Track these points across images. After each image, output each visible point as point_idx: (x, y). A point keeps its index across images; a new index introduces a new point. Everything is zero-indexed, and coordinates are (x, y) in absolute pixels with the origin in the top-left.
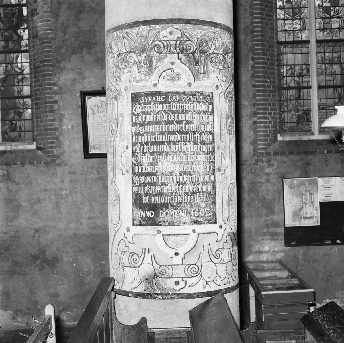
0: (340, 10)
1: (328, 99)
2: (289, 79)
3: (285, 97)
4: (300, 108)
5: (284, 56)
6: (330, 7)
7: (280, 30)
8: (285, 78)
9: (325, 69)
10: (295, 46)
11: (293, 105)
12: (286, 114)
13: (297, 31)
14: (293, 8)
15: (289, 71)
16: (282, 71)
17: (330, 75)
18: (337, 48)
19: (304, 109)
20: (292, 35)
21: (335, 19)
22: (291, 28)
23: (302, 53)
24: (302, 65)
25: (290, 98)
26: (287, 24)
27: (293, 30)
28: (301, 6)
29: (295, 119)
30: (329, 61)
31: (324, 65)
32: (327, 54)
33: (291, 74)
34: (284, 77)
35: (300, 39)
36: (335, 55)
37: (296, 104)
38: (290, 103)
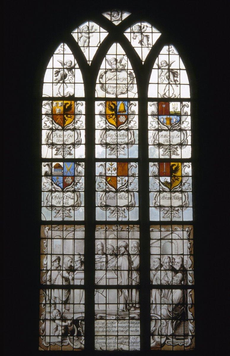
0: (130, 181)
1: (109, 304)
2: (55, 274)
3: (47, 299)
4: (69, 316)
5: (49, 241)
6: (117, 177)
7: (45, 205)
8: (50, 272)
9: (107, 262)
10: (64, 229)
11: (59, 311)
12: (48, 323)
13: (69, 208)
14: (64, 177)
16: (45, 262)
17: (113, 270)
18: (124, 234)
19: (75, 318)
20: (61, 212)
21: (123, 192)
23: (74, 239)
24: (74, 255)
25: (54, 301)
26: (56, 197)
27: (63, 207)
28: (76, 174)
29: (60, 331)
30: (113, 251)
31: (104, 256)
32: (110, 241)
33: (57, 267)
34: (47, 271)
35: (72, 219)
36: (121, 243)
37: (64, 310)
38: (55, 309)
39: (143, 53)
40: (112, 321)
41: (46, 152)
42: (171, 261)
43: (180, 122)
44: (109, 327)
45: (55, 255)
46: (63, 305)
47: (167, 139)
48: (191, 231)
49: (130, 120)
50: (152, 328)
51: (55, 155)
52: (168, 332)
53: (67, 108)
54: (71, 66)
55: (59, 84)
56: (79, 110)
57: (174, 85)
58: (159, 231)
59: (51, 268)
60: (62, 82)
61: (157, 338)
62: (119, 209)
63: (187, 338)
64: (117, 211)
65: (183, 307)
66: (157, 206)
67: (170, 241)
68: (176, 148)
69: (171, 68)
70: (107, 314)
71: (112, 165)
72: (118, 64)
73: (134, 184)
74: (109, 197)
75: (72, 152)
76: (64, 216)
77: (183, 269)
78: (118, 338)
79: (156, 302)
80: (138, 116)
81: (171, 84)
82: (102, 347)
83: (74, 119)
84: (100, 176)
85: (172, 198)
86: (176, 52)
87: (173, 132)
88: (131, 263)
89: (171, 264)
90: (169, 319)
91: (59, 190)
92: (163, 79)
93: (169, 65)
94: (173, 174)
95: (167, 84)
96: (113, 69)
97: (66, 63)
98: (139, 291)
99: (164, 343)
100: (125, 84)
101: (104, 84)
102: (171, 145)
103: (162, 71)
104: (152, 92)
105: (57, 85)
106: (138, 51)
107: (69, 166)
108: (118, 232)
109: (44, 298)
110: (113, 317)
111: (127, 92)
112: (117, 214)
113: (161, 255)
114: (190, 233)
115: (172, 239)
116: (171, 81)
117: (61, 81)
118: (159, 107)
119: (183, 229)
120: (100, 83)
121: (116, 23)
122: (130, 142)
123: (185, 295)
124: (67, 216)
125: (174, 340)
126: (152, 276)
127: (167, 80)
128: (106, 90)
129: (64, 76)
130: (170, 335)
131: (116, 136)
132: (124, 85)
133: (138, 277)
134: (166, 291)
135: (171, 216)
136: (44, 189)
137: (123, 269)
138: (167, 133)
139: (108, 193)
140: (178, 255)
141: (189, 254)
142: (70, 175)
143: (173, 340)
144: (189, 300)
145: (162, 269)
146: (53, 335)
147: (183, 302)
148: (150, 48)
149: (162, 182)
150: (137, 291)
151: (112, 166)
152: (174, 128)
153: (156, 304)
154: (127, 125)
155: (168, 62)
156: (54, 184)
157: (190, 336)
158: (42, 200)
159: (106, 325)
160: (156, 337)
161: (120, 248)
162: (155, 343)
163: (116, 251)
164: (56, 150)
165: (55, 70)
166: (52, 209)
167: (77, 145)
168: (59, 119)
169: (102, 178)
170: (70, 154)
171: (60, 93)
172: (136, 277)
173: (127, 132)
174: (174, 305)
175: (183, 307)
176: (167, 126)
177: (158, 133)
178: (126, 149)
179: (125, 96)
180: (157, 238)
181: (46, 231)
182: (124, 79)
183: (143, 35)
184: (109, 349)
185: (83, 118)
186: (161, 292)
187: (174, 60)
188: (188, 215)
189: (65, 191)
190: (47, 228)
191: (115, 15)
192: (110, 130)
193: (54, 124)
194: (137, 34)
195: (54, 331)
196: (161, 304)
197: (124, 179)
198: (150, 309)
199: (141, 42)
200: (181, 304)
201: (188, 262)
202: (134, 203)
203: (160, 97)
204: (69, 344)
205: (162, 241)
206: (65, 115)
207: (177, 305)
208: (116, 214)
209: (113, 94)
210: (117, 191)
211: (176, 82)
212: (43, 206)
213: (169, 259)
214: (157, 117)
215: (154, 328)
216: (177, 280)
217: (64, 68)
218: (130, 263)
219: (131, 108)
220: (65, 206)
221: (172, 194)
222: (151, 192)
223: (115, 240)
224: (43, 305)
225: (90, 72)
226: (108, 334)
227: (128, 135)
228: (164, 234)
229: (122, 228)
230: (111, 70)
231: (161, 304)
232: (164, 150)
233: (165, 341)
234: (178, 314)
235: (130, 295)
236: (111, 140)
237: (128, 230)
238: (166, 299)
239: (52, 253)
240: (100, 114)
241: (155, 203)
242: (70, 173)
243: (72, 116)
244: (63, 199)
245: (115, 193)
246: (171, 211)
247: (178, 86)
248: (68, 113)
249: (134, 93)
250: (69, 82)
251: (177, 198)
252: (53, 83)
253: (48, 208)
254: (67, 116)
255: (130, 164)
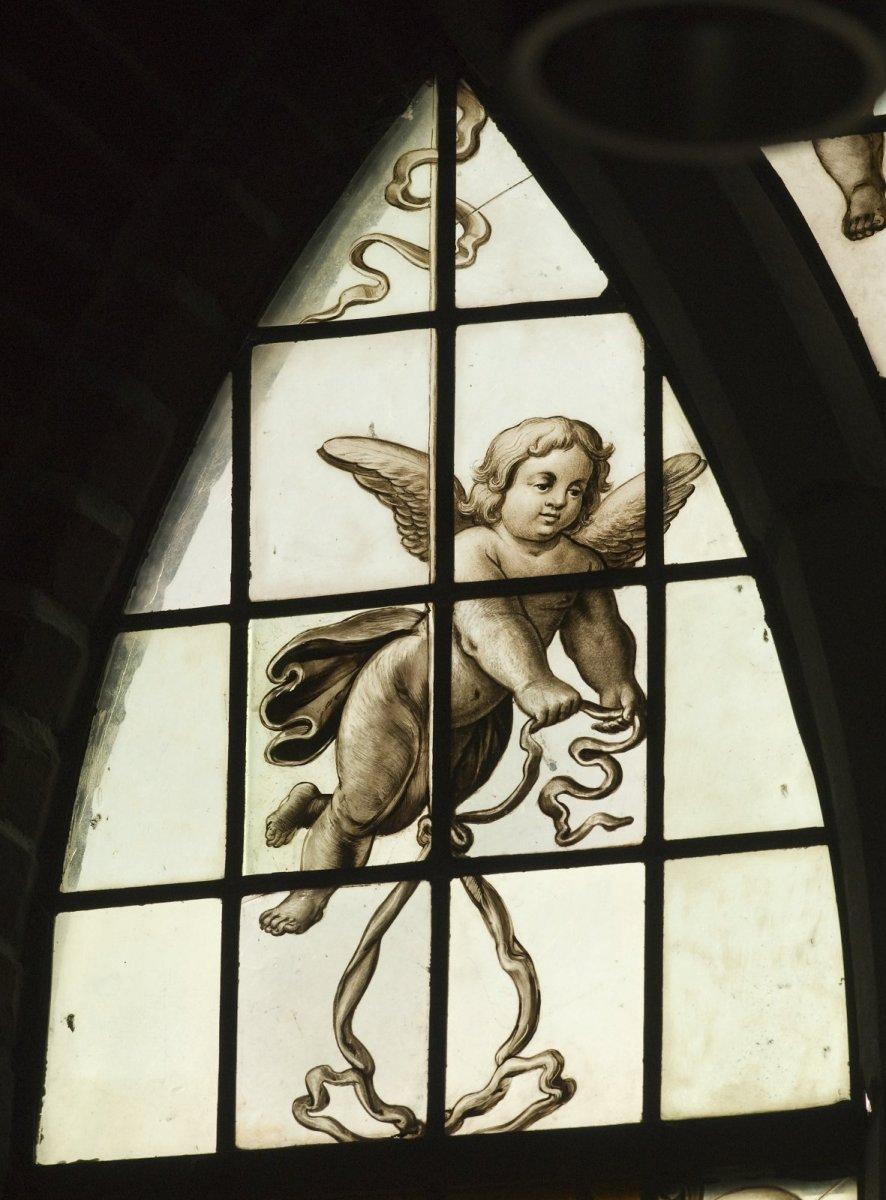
54: (590, 534)
55: (354, 905)
60: (402, 847)
97: (487, 473)
117: (391, 824)
129: (463, 735)
165: (270, 638)
171: (365, 1075)
217: (444, 592)
250: (547, 844)
252: (232, 888)
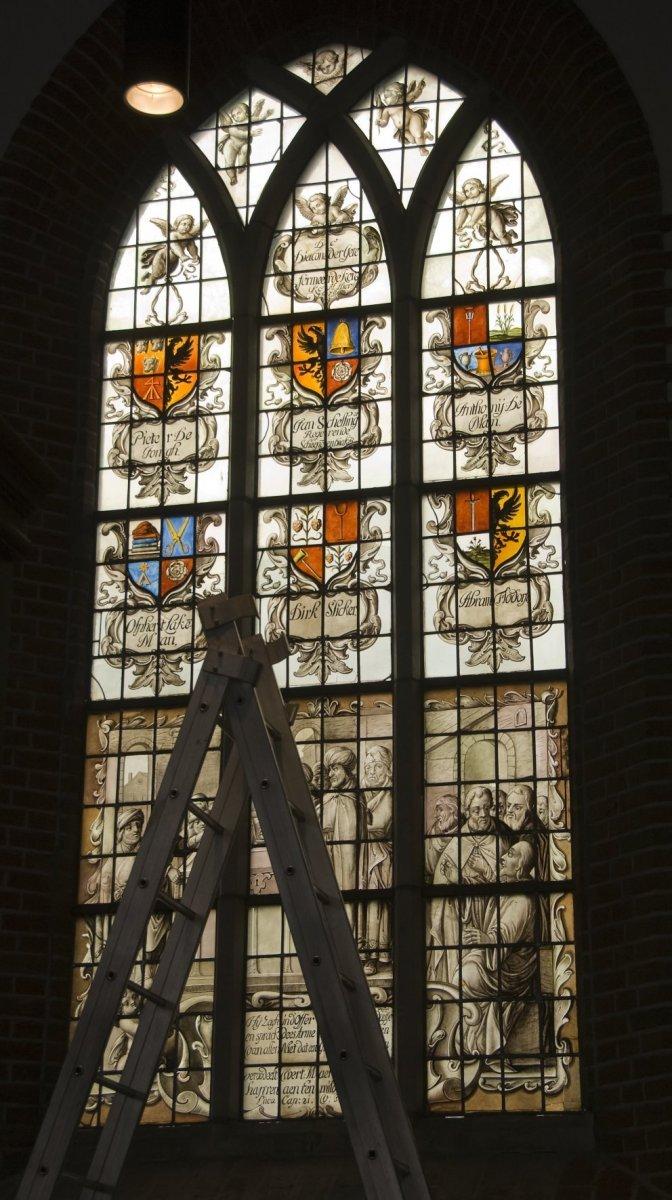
0: (365, 557)
7: (104, 651)
8: (110, 860)
10: (160, 719)
13: (175, 657)
15: (127, 832)
18: (344, 726)
20: (152, 670)
21: (342, 596)
22: (148, 643)
26: (137, 625)
27: (158, 653)
36: (334, 754)
39: (406, 168)
40: (301, 1013)
41: (114, 492)
42: (492, 803)
43: (522, 359)
44: (290, 1035)
45: (129, 808)
46: (147, 968)
47: (481, 416)
48: (560, 700)
49: (367, 372)
50: (433, 1033)
51: (139, 496)
52: (485, 1045)
53: (175, 352)
54: (191, 232)
55: (154, 290)
56: (214, 357)
57: (504, 249)
58: (454, 708)
59: (115, 848)
60: (162, 281)
61: (450, 1069)
62: (329, 646)
63: (554, 1062)
64: (323, 654)
65: (535, 956)
66: (448, 628)
67: (491, 736)
68: (510, 444)
69: (494, 199)
70: (285, 990)
71: (310, 512)
72: (333, 211)
73: (380, 564)
74: (298, 612)
75: (189, 484)
76: (161, 682)
77: (535, 825)
78: (318, 1070)
79: (443, 942)
80: (389, 357)
81: (494, 248)
82: (265, 1106)
83: (197, 384)
84: (273, 548)
85: (497, 600)
86: (512, 148)
87: (499, 392)
88: (365, 818)
89: (492, 813)
90: (489, 1000)
91: (147, 603)
92: (470, 235)
93: (488, 190)
94: (501, 522)
95: (482, 249)
96: (317, 228)
97: (176, 223)
98: (388, 909)
99: (474, 1085)
100: (350, 267)
101: (288, 274)
102: (495, 433)
103: (467, 214)
104: (436, 282)
105: (148, 292)
106: (391, 161)
107: (176, 534)
108: (326, 719)
109: (88, 946)
110: (303, 1001)
111: (359, 291)
112: (323, 661)
113: (459, 783)
114: (556, 708)
115: (495, 731)
116: (495, 237)
117: (160, 277)
118: (456, 322)
119: (532, 693)
120: (278, 273)
121: (326, 89)
122: (365, 441)
123: (543, 914)
124: (169, 682)
125: (509, 1074)
126: (430, 853)
127: (481, 238)
128: (292, 291)
129: (172, 263)
130: (493, 1057)
131: (321, 426)
132: (349, 271)
133: (388, 862)
134: (479, 904)
135: (495, 657)
136: (102, 602)
137: (338, 840)
138: (482, 399)
139: (294, 599)
140: (516, 780)
141: (553, 775)
142: (183, 554)
143: (503, 1073)
144: (557, 930)
145: (465, 829)
146: (112, 1068)
147: (535, 938)
148: (430, 149)
149: (464, 554)
150: (382, 908)
151: (310, 516)
152: (504, 381)
153: (444, 948)
154: (357, 388)
155: (484, 182)
156: (133, 587)
157: (562, 1055)
158: (96, 638)
159: (281, 1028)
160: (446, 1065)
161: (329, 770)
162: (441, 1085)
163: (317, 780)
164: (140, 483)
165: (142, 250)
166: (124, 664)
167: (203, 463)
168: (152, 388)
169: (276, 555)
170: (183, 490)
171: (156, 316)
172: (378, 865)
173: (357, 411)
174: (505, 949)
175: (535, 956)
176: (480, 378)
177: (452, 402)
178: (353, 463)
179: (350, 302)
180: (448, 731)
181: (103, 733)
182: (349, 253)
183: (411, 111)
184: (288, 1110)
185: (224, 381)
186: (460, 905)
187: (503, 173)
188: (550, 650)
189: (166, 605)
190: (107, 723)
191: (327, 63)
192: (303, 408)
193: (137, 405)
194: (392, 110)
195: (115, 1055)
196: (460, 947)
197: (346, 552)
198: (423, 967)
199: (402, 133)
200: (528, 946)
201: (553, 803)
202: (376, 624)
203: (459, 292)
204: (160, 1098)
205: (464, 739)
206: (170, 374)
207: (514, 948)
208: (319, 664)
209: (315, 300)
210: (324, 590)
211: (510, 240)
212: (99, 657)
213: (485, 797)
214: (448, 352)
215: (439, 1033)
216: (514, 865)
217: (169, 242)
218: (363, 815)
219: (369, 335)
220: (164, 652)
221: (496, 587)
222: (428, 585)
223: (313, 746)
224: (82, 969)
225: (250, 247)
226: (286, 1057)
227: (359, 418)
228: (471, 716)
229: (338, 707)
230: (309, 230)
231: (460, 947)
232: (472, 452)
233: (478, 1076)
234: (518, 977)
235: (359, 923)
236: (308, 439)
237: (355, 710)
238: (479, 928)
239: (121, 800)
240: (275, 364)
241: (442, 620)
242: (180, 550)
243: (190, 377)
244: (159, 629)
245: (317, 598)
246: (494, 643)
247: (515, 251)
248: (181, 367)
249: (378, 290)
250: (184, 280)
251: (511, 598)
252: (136, 288)
253: (112, 660)
254: (175, 378)
255: (365, 504)
